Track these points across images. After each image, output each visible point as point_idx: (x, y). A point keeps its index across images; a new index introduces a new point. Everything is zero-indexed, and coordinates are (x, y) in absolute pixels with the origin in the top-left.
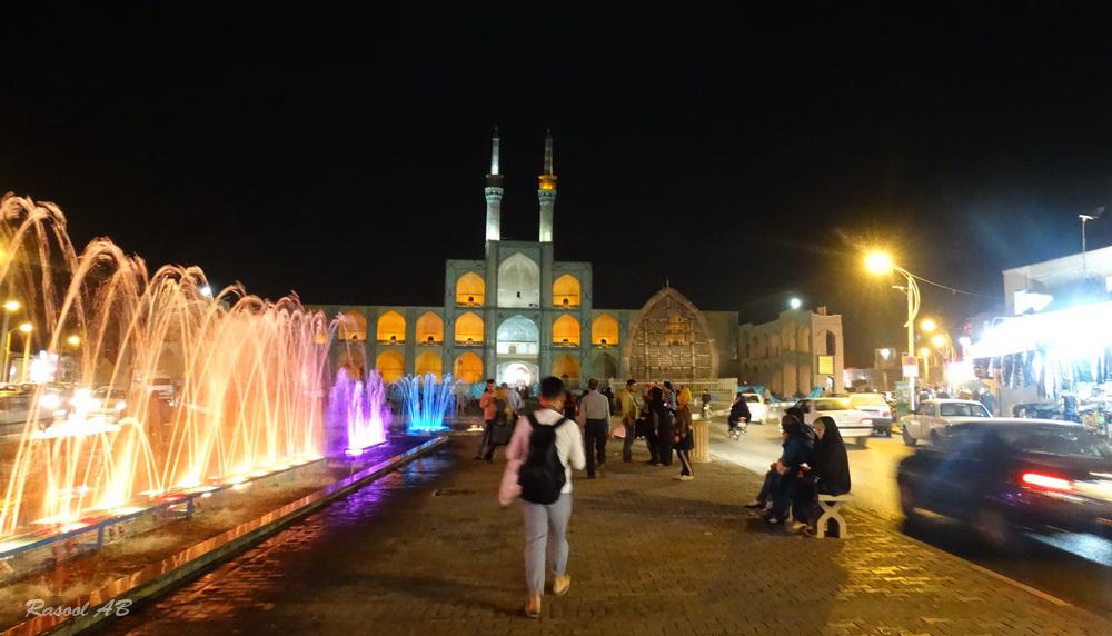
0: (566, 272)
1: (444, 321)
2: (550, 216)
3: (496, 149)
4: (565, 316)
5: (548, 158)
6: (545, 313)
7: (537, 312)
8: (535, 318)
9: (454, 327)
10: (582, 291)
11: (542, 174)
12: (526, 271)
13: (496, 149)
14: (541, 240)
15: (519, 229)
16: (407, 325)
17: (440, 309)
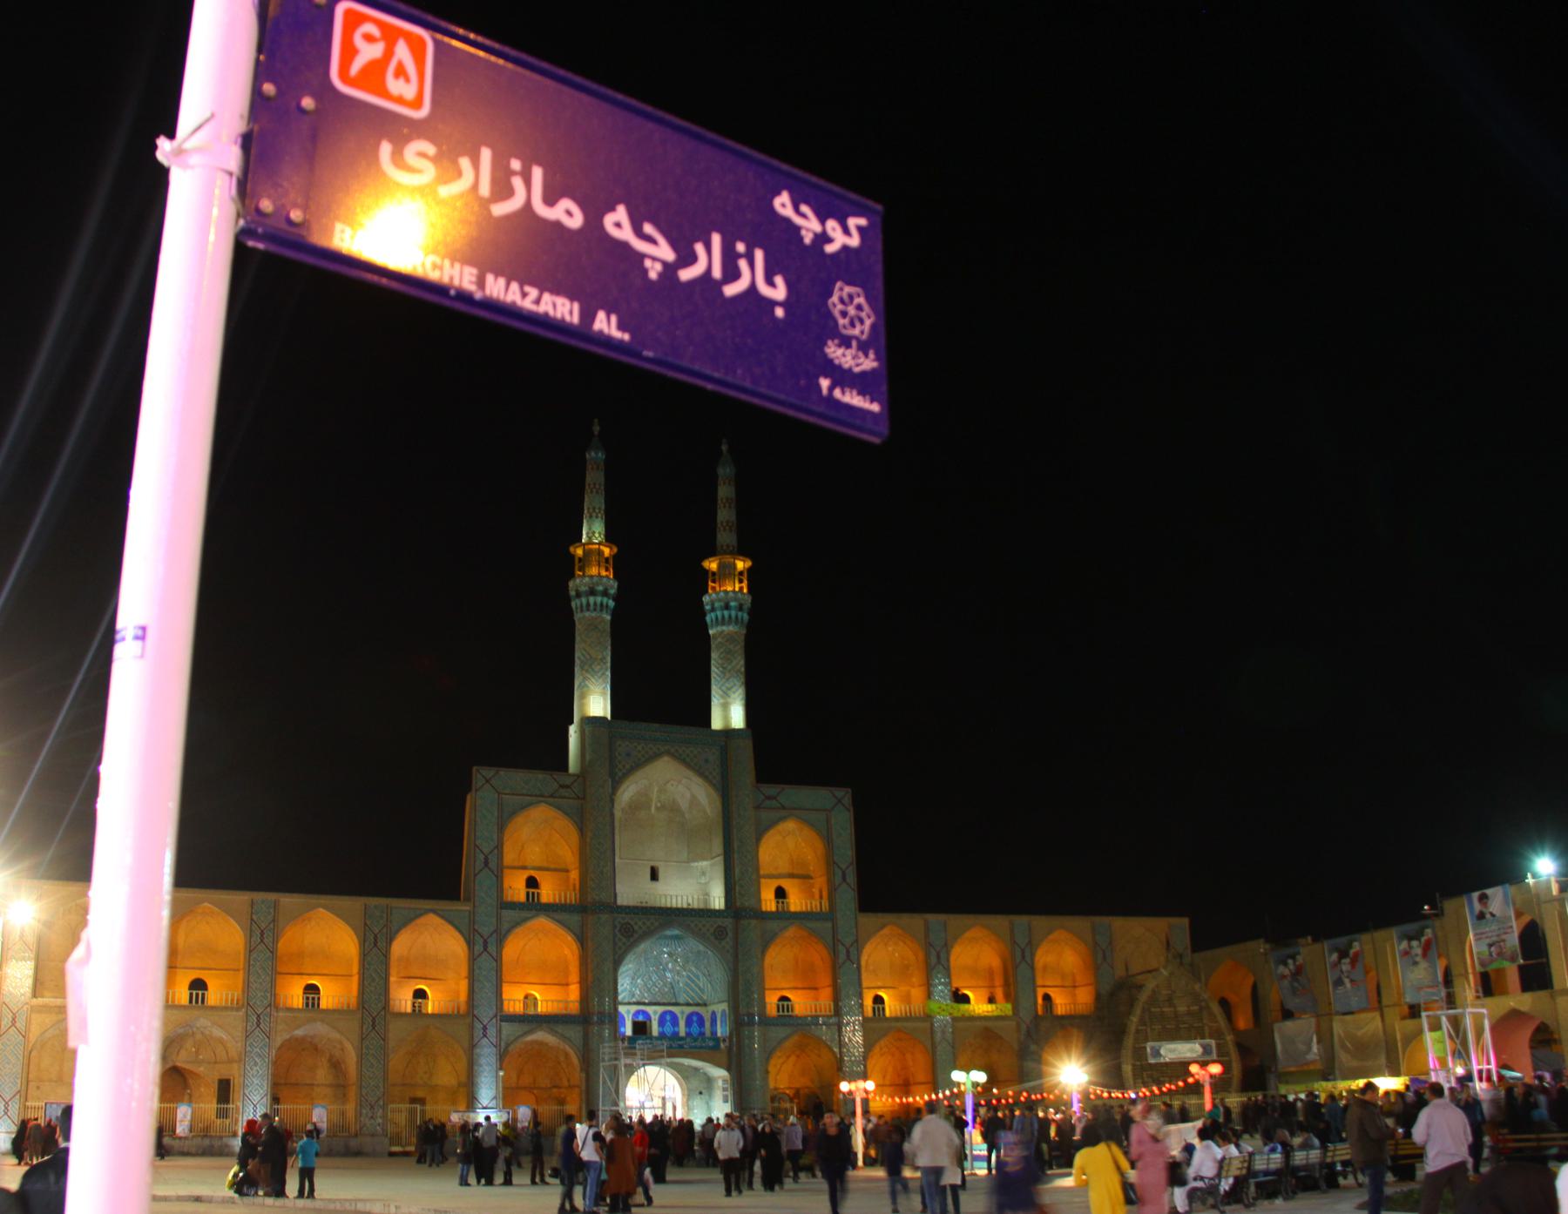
0: (787, 811)
1: (470, 943)
2: (740, 663)
3: (595, 478)
4: (791, 931)
5: (725, 514)
6: (744, 922)
7: (719, 922)
8: (720, 934)
9: (498, 959)
10: (830, 862)
11: (712, 552)
12: (672, 808)
13: (595, 478)
14: (717, 723)
15: (661, 695)
16: (364, 956)
17: (463, 907)
